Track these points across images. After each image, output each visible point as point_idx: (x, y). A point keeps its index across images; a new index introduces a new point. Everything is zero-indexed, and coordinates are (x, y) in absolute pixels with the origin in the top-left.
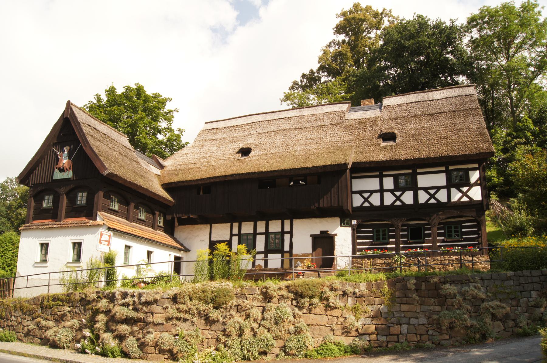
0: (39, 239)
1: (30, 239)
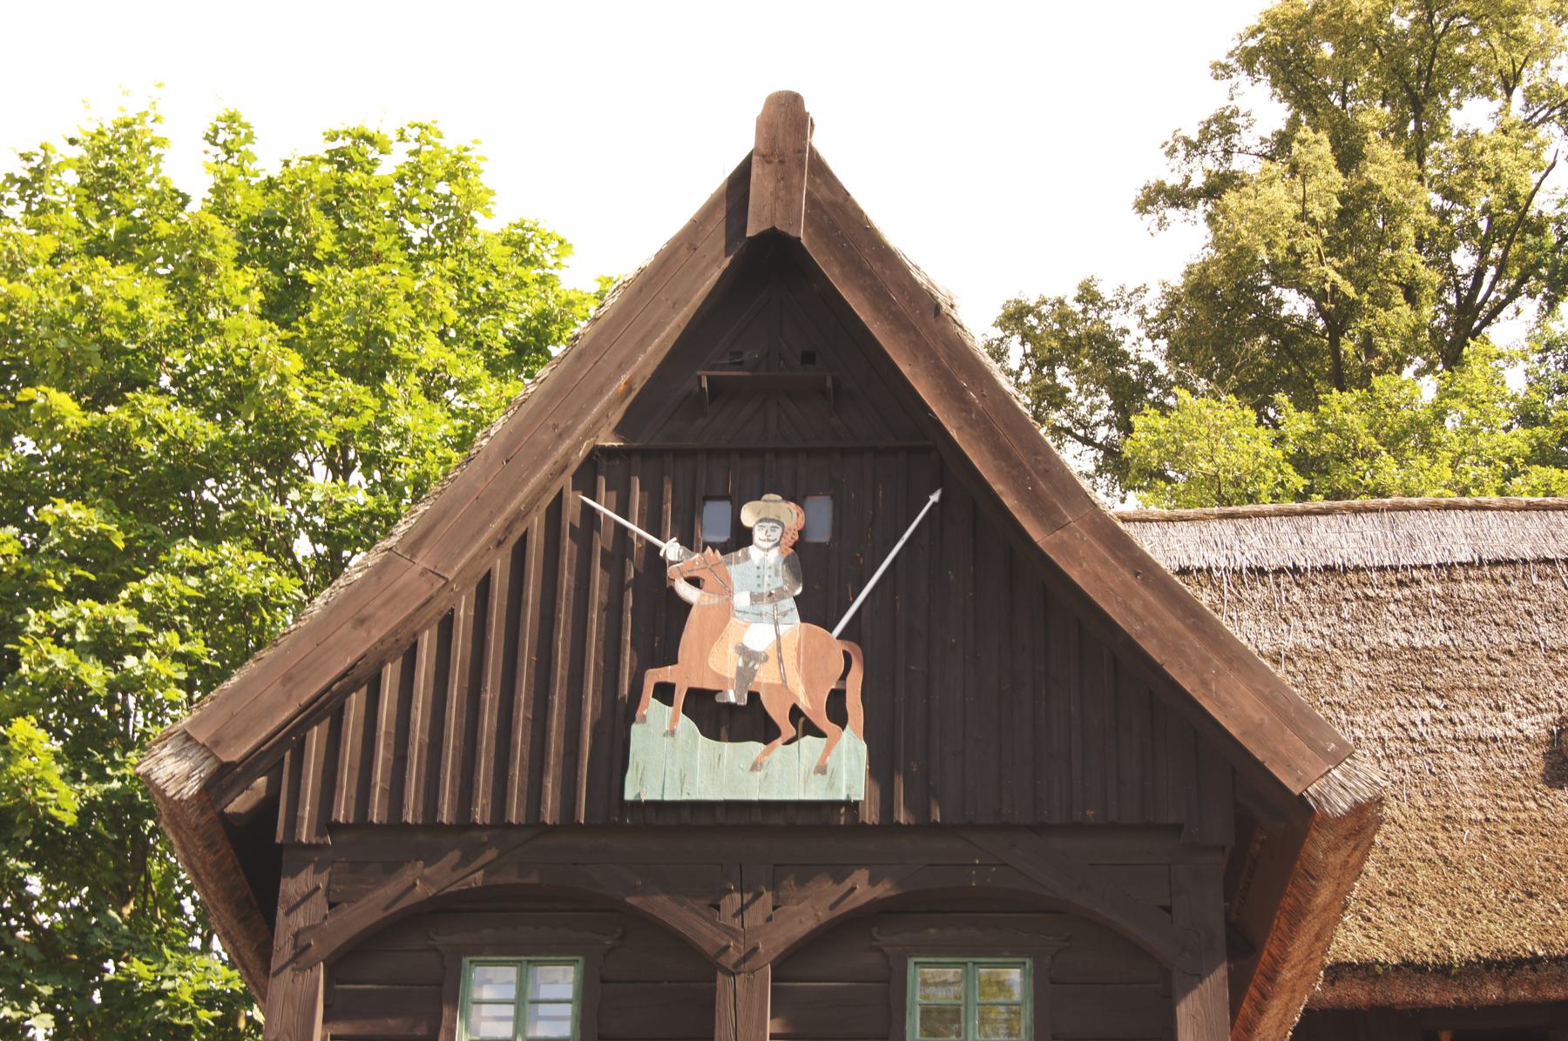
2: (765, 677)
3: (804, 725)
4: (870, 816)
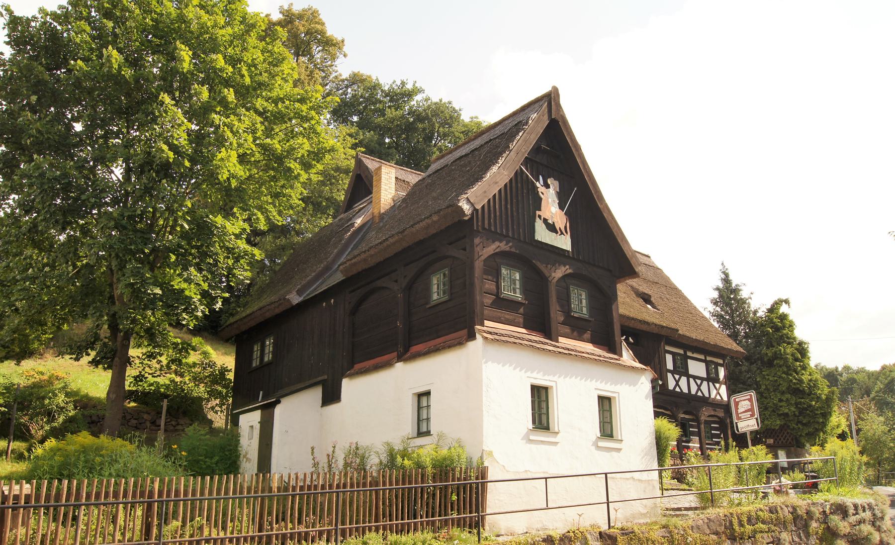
0: (529, 374)
1: (508, 369)
2: (555, 220)
3: (562, 233)
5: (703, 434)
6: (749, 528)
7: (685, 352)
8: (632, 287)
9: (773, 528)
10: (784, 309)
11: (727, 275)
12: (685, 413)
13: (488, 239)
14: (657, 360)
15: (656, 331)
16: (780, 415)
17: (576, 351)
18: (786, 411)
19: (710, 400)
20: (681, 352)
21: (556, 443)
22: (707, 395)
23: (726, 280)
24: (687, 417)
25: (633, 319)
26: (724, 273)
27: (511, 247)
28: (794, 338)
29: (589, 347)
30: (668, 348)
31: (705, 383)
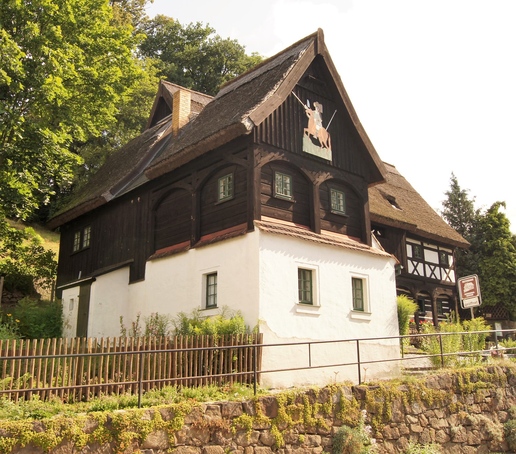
0: (296, 259)
2: (319, 136)
3: (324, 146)
4: (331, 164)
5: (435, 309)
6: (471, 385)
7: (422, 244)
8: (380, 191)
9: (491, 384)
10: (501, 210)
11: (456, 182)
12: (422, 292)
13: (265, 150)
14: (399, 250)
15: (398, 226)
16: (497, 295)
17: (335, 241)
18: (502, 292)
19: (441, 282)
20: (419, 243)
21: (317, 315)
22: (439, 278)
23: (455, 186)
24: (423, 295)
25: (380, 216)
26: (453, 180)
27: (283, 157)
28: (509, 233)
29: (345, 238)
30: (408, 240)
31: (438, 268)
